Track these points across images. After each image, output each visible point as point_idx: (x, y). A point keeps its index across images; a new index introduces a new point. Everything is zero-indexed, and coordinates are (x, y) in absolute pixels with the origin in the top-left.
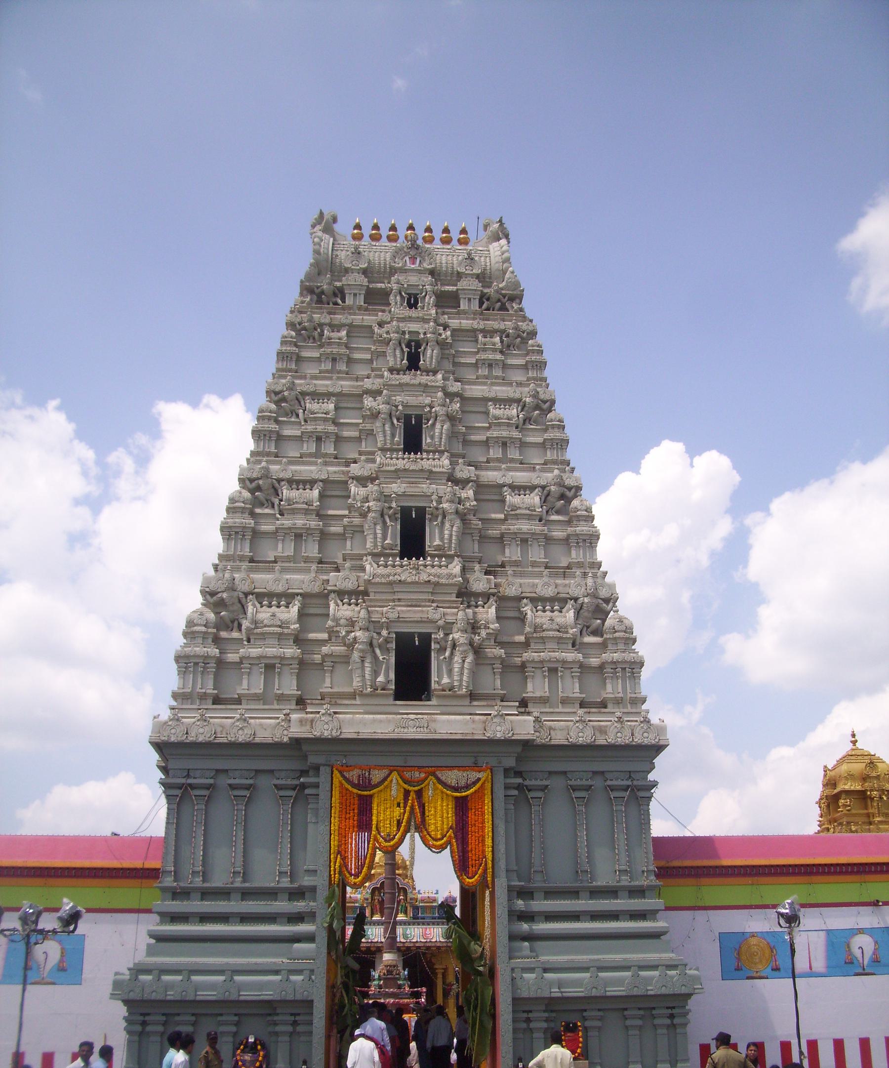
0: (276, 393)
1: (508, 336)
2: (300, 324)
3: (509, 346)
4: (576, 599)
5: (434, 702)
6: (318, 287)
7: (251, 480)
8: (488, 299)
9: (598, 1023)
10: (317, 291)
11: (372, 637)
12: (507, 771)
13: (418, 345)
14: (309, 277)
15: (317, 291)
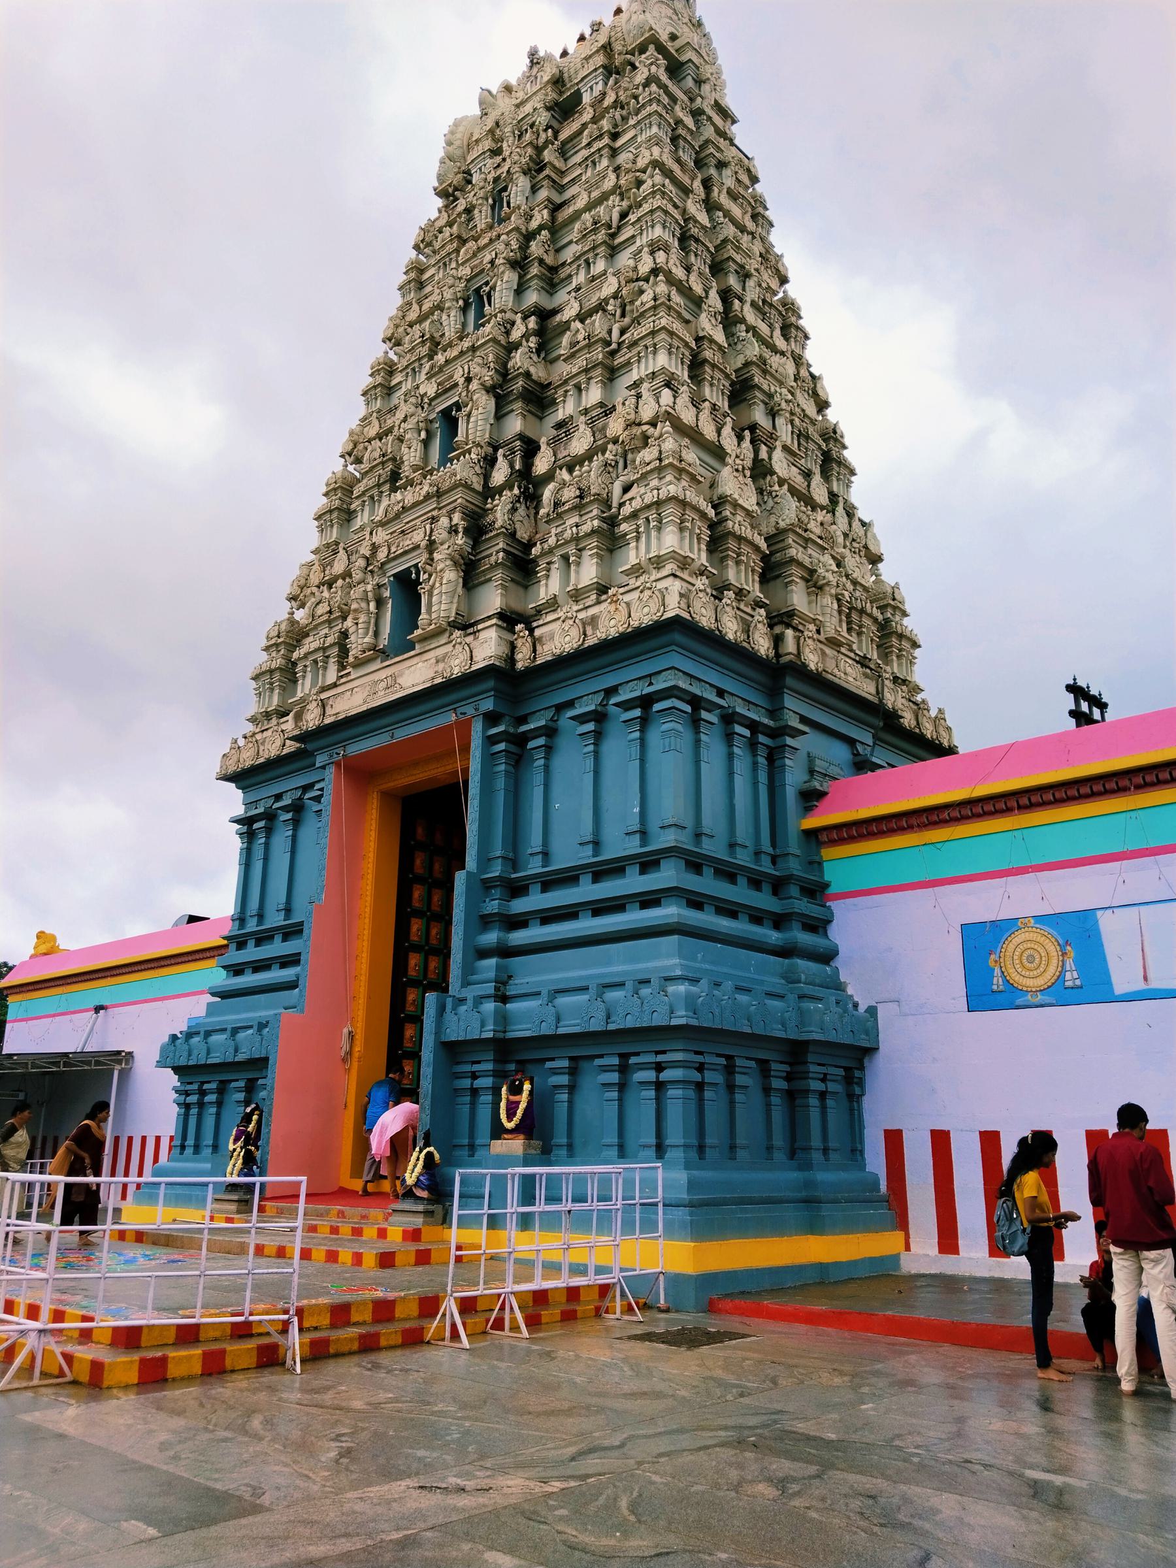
0: (390, 339)
1: (622, 108)
2: (422, 241)
3: (625, 119)
4: (615, 441)
5: (418, 648)
6: (450, 185)
7: (350, 454)
8: (618, 73)
9: (564, 1080)
10: (450, 190)
11: (365, 592)
12: (491, 718)
13: (505, 189)
14: (441, 178)
15: (450, 190)
